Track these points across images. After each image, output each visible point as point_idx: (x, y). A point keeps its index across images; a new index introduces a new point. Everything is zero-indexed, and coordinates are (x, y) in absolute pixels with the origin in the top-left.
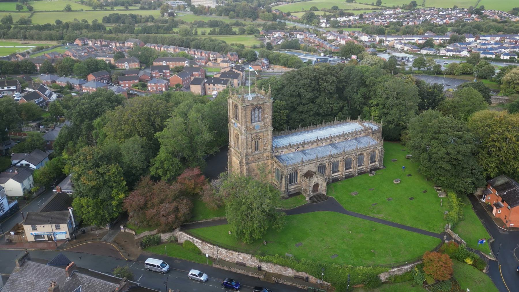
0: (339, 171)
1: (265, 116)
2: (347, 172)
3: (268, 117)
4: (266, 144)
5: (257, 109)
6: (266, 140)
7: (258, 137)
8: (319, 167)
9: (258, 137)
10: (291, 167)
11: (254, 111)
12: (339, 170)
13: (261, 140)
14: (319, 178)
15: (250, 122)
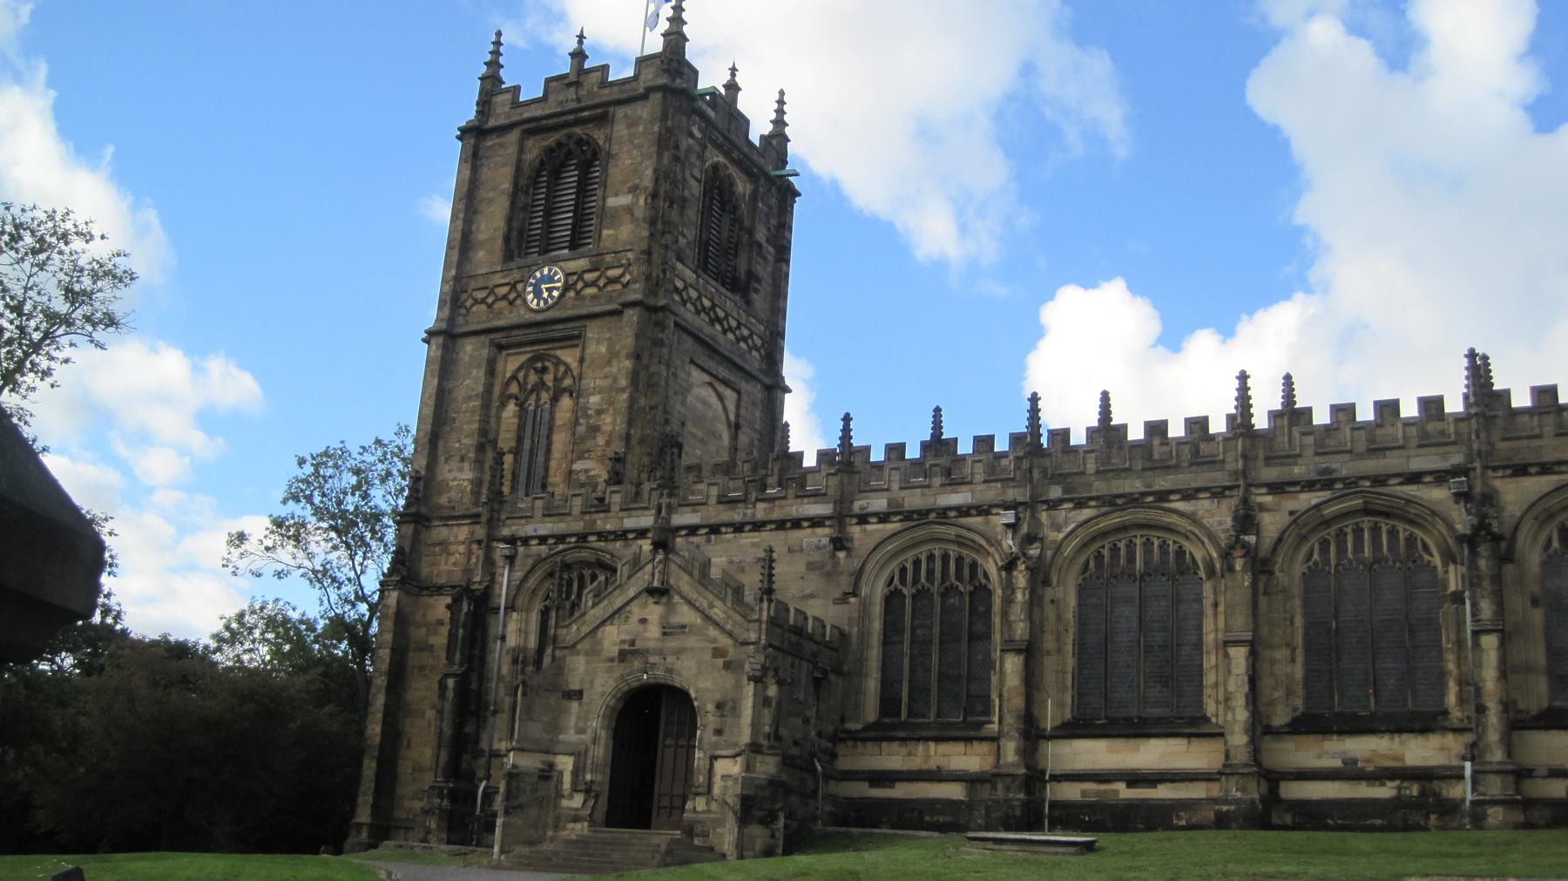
0: (1192, 725)
1: (612, 202)
2: (1350, 772)
3: (629, 210)
4: (594, 430)
5: (571, 177)
6: (594, 399)
7: (549, 378)
8: (892, 600)
9: (549, 378)
10: (546, 528)
11: (557, 174)
12: (1210, 708)
13: (566, 402)
14: (685, 615)
15: (499, 243)
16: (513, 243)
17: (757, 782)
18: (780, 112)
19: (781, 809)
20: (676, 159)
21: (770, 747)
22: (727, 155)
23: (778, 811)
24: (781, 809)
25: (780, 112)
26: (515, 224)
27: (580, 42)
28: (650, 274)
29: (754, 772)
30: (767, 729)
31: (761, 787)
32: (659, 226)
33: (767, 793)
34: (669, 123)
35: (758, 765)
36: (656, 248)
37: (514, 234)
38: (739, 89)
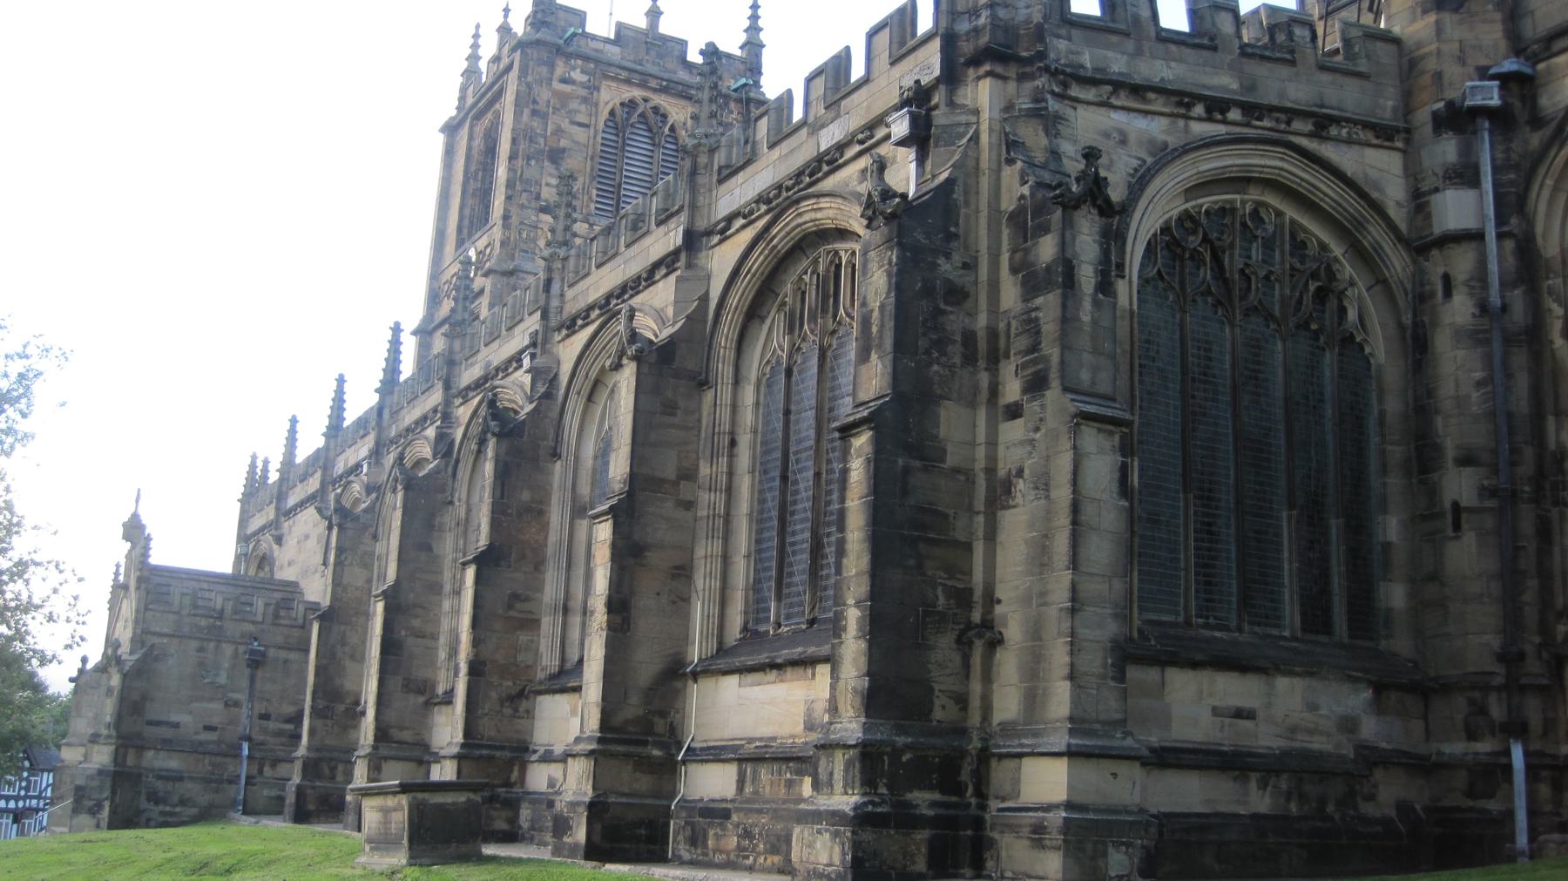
16: (465, 231)
17: (89, 772)
18: (754, 17)
19: (106, 799)
20: (534, 113)
21: (109, 737)
22: (643, 85)
23: (104, 800)
24: (106, 799)
25: (754, 17)
26: (467, 212)
27: (506, 16)
28: (509, 238)
29: (91, 762)
30: (108, 719)
31: (90, 777)
32: (519, 187)
33: (95, 783)
34: (530, 79)
35: (95, 754)
36: (514, 210)
37: (466, 222)
38: (661, 13)
